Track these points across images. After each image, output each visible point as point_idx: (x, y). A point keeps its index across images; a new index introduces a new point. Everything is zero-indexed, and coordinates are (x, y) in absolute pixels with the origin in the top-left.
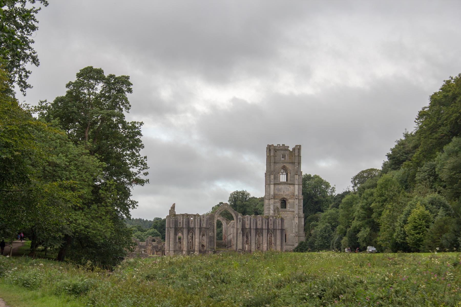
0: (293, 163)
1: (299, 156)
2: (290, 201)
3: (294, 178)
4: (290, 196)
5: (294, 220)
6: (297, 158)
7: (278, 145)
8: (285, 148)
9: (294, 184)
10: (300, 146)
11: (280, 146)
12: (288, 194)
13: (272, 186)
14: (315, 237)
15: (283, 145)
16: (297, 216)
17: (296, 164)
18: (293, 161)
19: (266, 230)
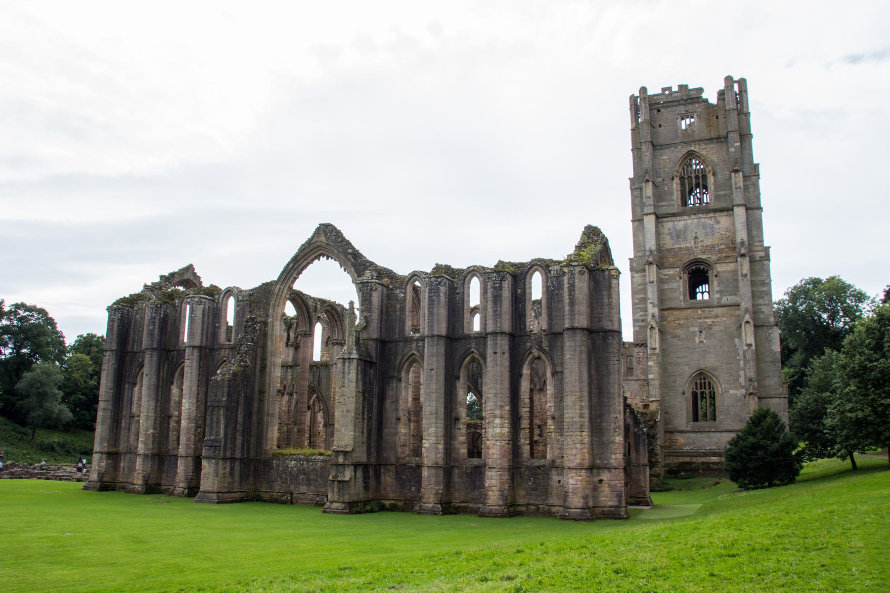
0: (722, 140)
1: (743, 114)
2: (720, 268)
3: (730, 187)
4: (720, 251)
5: (740, 337)
6: (734, 116)
7: (664, 90)
8: (688, 98)
9: (728, 210)
10: (742, 82)
11: (671, 93)
12: (713, 247)
13: (650, 222)
14: (825, 386)
15: (683, 87)
16: (747, 317)
17: (734, 137)
18: (723, 133)
19: (504, 343)
